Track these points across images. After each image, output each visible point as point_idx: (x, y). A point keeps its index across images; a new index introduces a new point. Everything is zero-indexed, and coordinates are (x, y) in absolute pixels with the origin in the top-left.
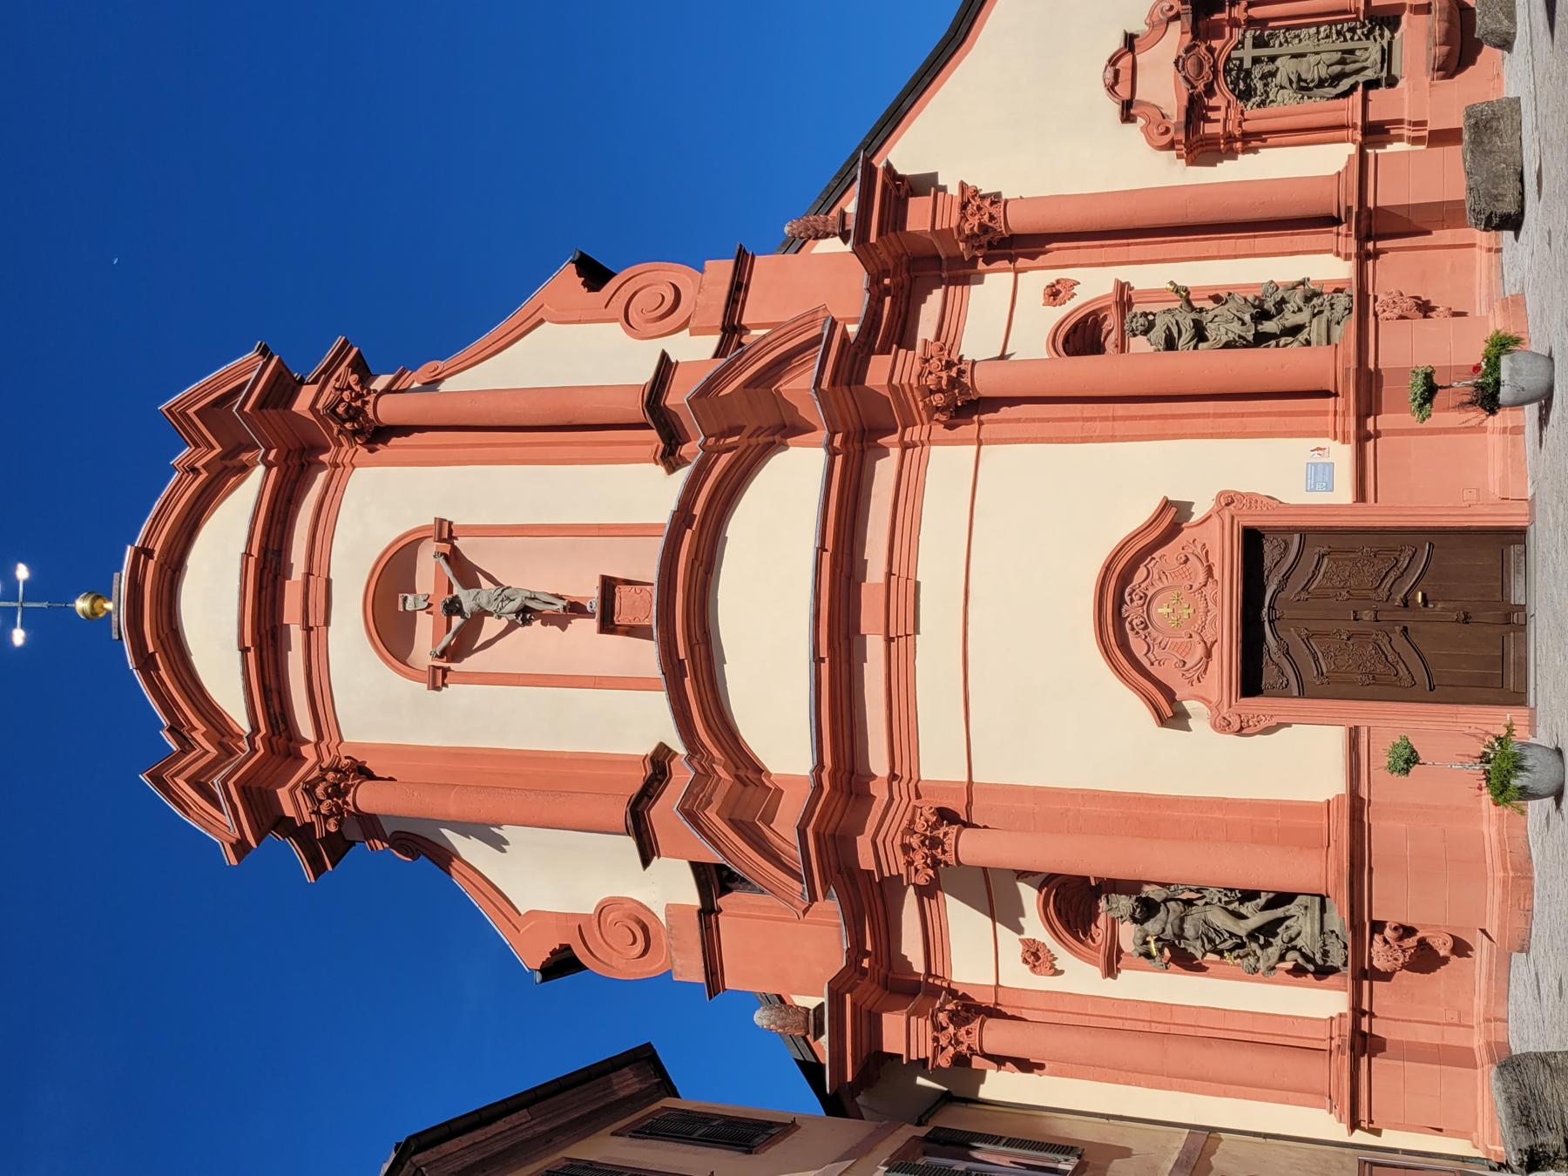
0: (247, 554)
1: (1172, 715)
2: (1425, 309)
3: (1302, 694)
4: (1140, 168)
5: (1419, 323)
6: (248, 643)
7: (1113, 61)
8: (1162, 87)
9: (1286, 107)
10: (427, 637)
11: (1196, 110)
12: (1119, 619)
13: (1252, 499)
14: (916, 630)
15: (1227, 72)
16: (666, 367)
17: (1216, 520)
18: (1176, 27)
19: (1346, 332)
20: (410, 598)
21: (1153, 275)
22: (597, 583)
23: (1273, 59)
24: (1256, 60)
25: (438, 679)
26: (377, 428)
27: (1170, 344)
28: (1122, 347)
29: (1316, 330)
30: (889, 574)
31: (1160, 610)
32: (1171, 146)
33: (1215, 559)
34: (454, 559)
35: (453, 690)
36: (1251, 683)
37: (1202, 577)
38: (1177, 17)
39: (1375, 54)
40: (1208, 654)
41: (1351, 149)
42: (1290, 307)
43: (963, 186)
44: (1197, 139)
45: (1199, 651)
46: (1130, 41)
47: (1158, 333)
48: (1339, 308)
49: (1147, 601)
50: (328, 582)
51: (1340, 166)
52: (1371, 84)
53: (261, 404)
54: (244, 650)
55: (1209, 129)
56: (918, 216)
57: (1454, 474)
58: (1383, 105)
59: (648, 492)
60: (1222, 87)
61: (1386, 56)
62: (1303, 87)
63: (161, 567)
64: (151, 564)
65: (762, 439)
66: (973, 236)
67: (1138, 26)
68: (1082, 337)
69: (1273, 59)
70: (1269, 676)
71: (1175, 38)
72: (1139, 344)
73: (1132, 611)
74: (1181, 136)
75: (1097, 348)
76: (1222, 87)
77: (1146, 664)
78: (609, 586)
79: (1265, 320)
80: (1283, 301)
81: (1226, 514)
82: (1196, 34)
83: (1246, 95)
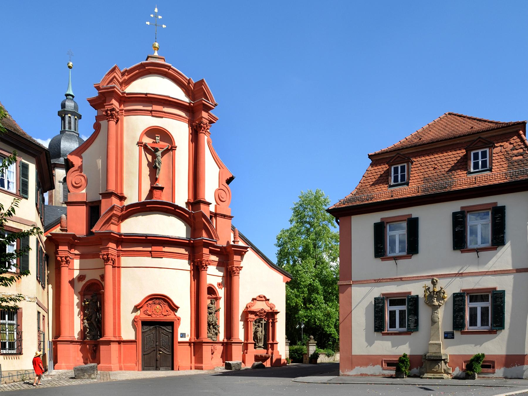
0: (169, 97)
1: (136, 308)
2: (212, 354)
3: (142, 332)
4: (243, 301)
5: (211, 353)
6: (148, 95)
7: (264, 297)
8: (259, 306)
9: (252, 329)
10: (147, 141)
11: (253, 313)
12: (156, 298)
13: (179, 324)
14: (153, 257)
15: (260, 318)
16: (209, 204)
17: (174, 317)
18: (269, 308)
19: (209, 340)
20: (159, 138)
21: (222, 304)
22: (163, 186)
23: (262, 327)
24: (262, 324)
25: (139, 144)
26: (197, 132)
27: (209, 308)
28: (208, 298)
29: (210, 335)
30: (165, 252)
31: (158, 306)
32: (247, 307)
33: (168, 317)
34: (167, 151)
35: (137, 148)
36: (145, 323)
37: (164, 314)
38: (271, 309)
39: (260, 345)
40: (149, 315)
41: (243, 341)
42: (214, 330)
43: (242, 267)
44: (247, 313)
45: (150, 314)
46: (268, 300)
47: (211, 305)
48: (214, 339)
49: (159, 304)
50: (162, 117)
51: (240, 339)
52: (255, 344)
53: (204, 104)
54: (146, 94)
55: (249, 315)
56: (236, 258)
57: (183, 355)
58: (251, 347)
59: (181, 199)
60: (257, 318)
61: (260, 347)
62: (256, 332)
63: (167, 72)
64: (167, 70)
65: (193, 224)
66: (232, 269)
67: (270, 302)
68: (211, 290)
69: (262, 327)
70: (145, 327)
71: (267, 309)
72: (209, 301)
73: (157, 301)
74: (249, 310)
75: (209, 293)
76: (257, 318)
77: (147, 303)
78: (162, 189)
79: (213, 325)
80: (216, 329)
81: (176, 319)
82: (268, 313)
83: (256, 322)
